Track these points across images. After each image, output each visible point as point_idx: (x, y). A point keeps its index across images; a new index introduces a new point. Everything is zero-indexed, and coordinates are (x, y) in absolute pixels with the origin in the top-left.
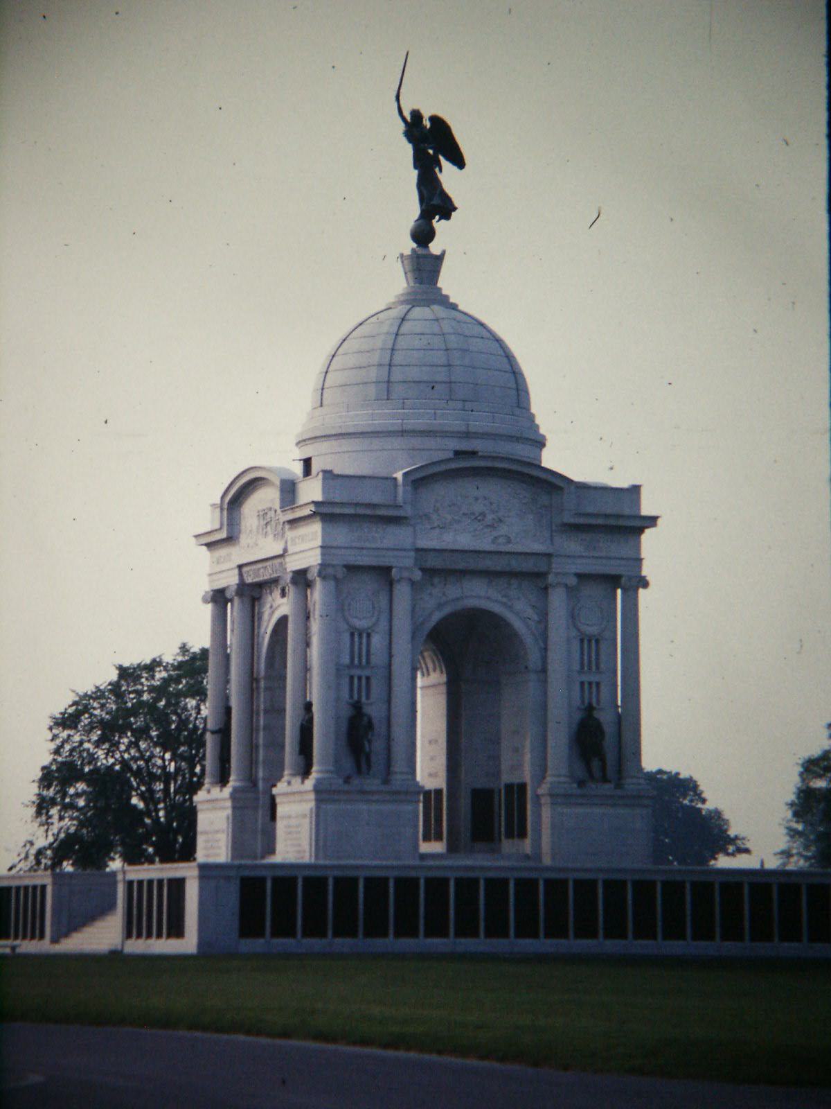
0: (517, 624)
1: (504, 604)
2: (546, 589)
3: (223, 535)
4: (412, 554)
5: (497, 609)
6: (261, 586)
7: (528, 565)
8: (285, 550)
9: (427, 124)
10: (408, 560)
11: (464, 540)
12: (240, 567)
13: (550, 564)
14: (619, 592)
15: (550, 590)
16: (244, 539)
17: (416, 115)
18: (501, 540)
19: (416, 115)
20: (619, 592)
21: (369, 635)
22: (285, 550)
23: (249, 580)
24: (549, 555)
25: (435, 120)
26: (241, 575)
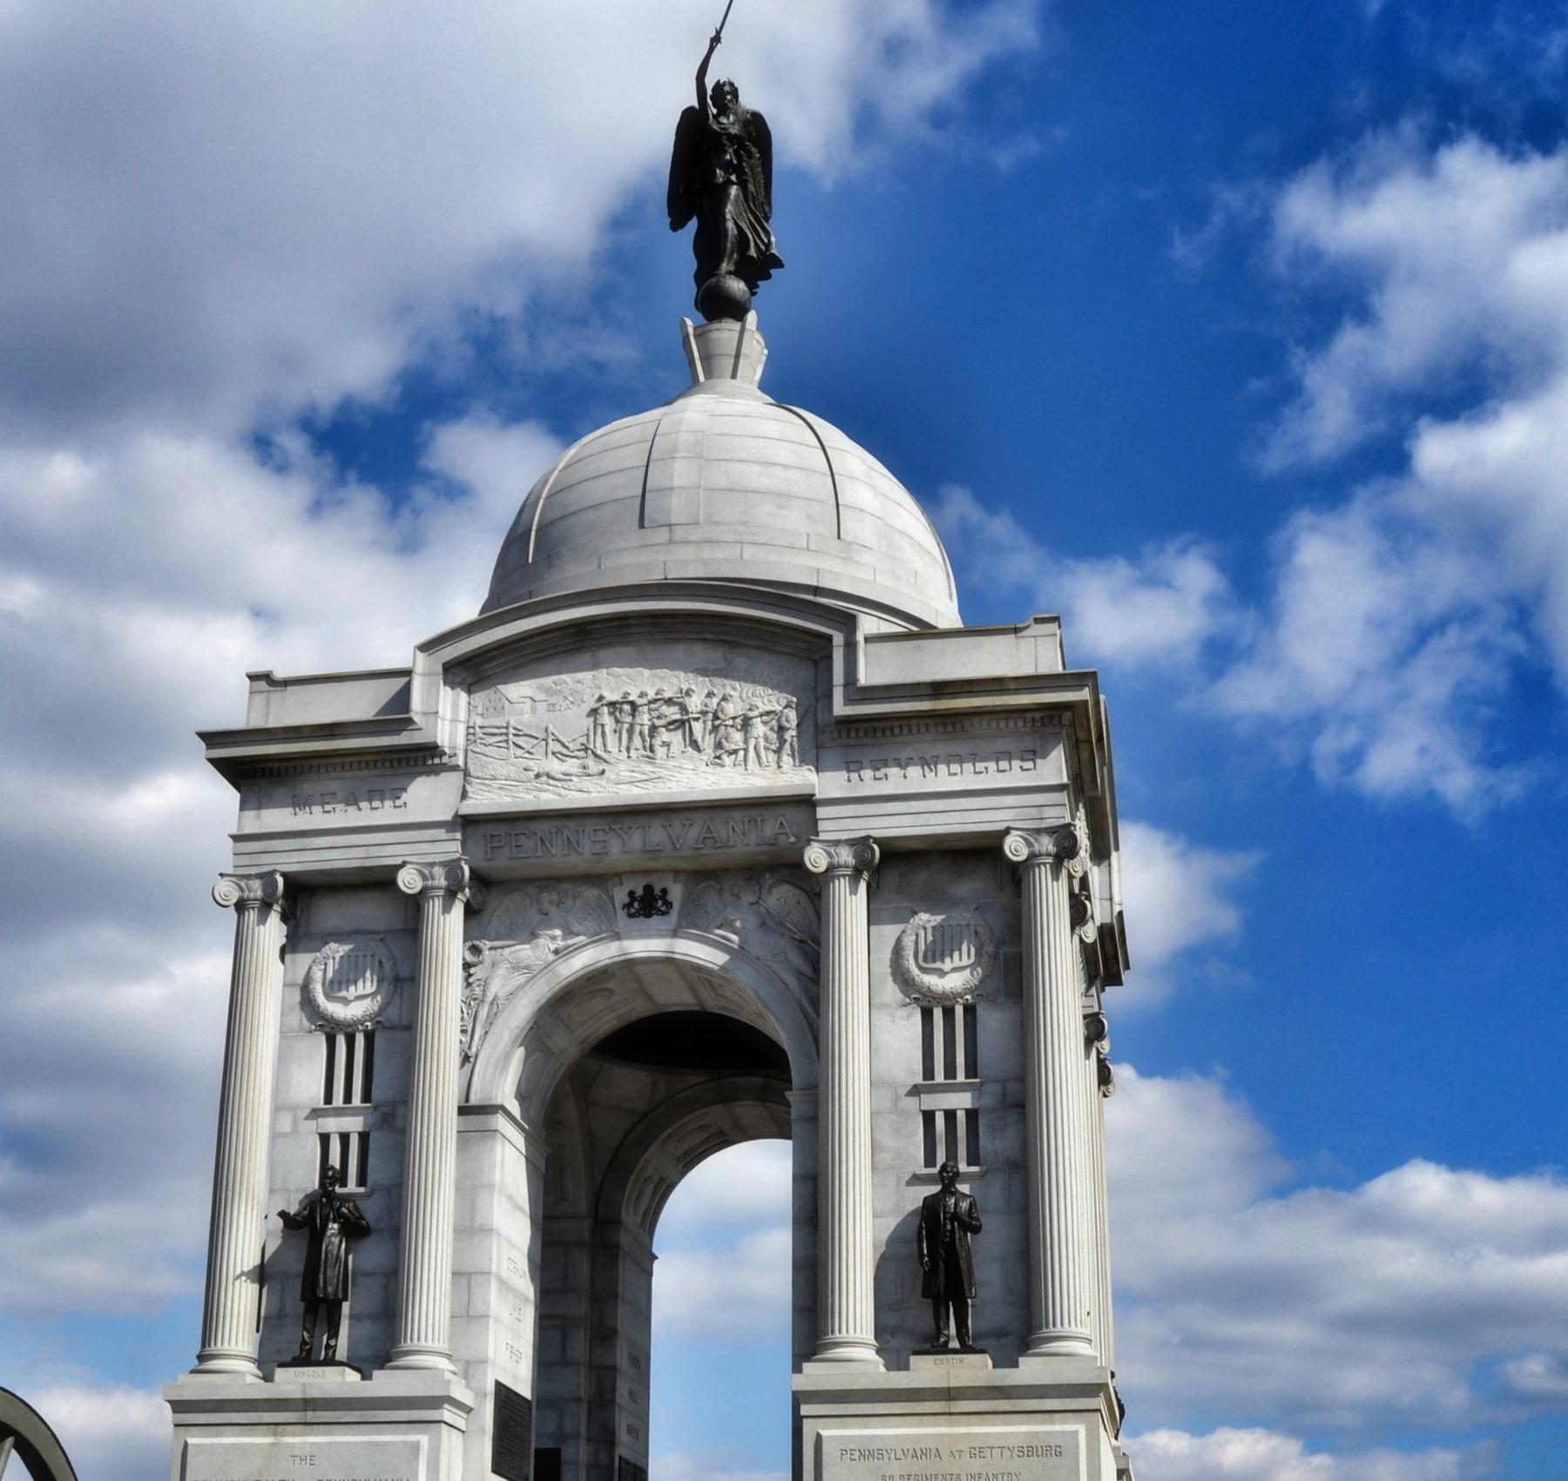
17: (724, 95)
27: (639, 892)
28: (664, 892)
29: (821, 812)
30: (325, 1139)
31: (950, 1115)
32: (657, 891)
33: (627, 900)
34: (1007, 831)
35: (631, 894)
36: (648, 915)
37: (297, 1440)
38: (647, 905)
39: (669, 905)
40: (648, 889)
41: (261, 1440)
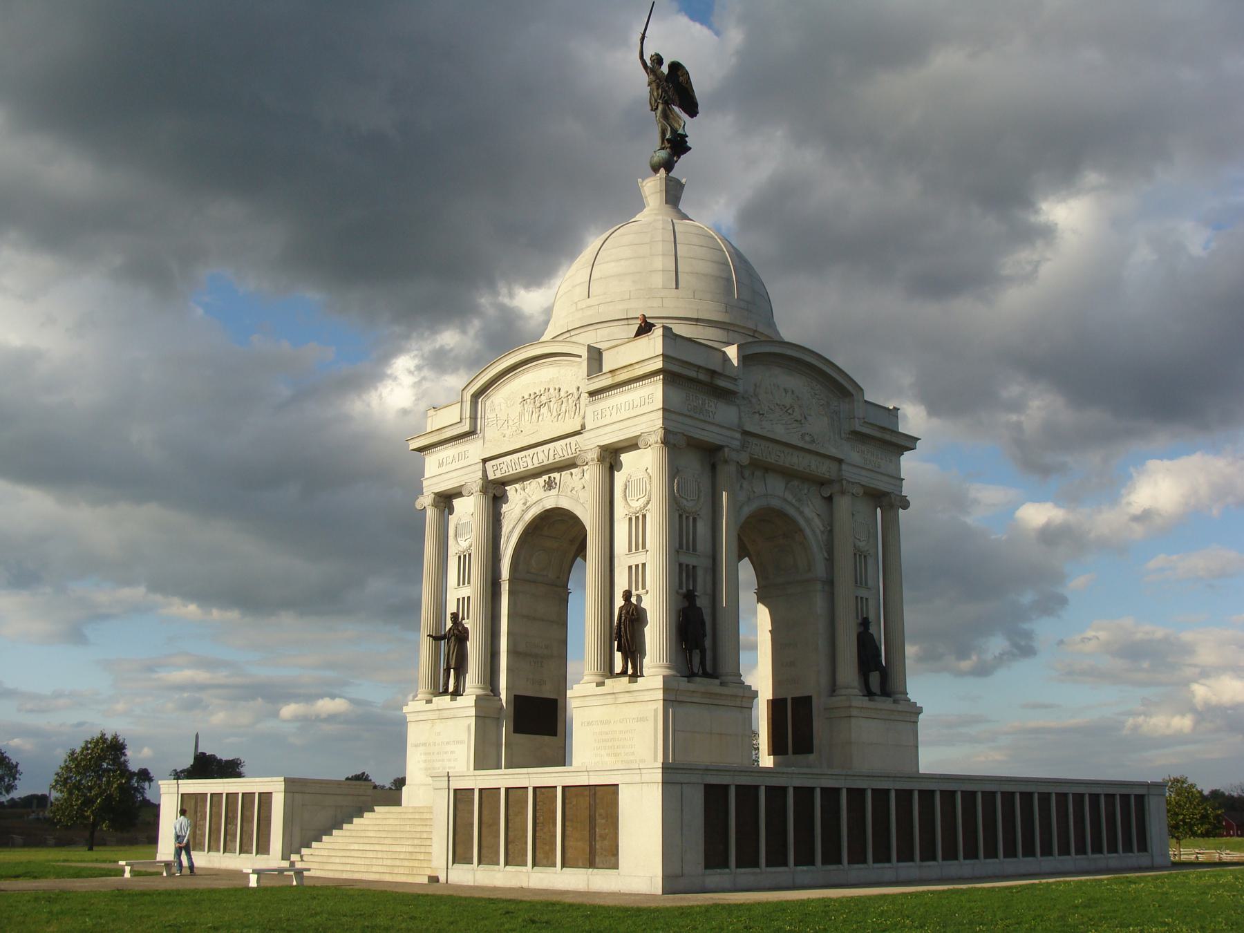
0: (808, 532)
1: (798, 509)
2: (830, 499)
3: (466, 427)
4: (738, 436)
5: (791, 511)
6: (503, 483)
7: (824, 469)
8: (583, 427)
9: (665, 69)
10: (735, 440)
11: (780, 432)
12: (485, 461)
13: (840, 470)
14: (879, 510)
15: (834, 500)
16: (490, 433)
17: (658, 60)
18: (807, 438)
19: (658, 60)
20: (879, 510)
21: (694, 520)
22: (583, 427)
23: (491, 476)
24: (840, 461)
25: (676, 67)
26: (485, 472)
27: (547, 480)
28: (554, 478)
29: (586, 435)
30: (458, 599)
31: (637, 566)
32: (552, 479)
33: (544, 484)
34: (639, 436)
35: (545, 481)
36: (550, 490)
37: (439, 726)
38: (550, 485)
39: (556, 484)
40: (549, 477)
41: (429, 724)
